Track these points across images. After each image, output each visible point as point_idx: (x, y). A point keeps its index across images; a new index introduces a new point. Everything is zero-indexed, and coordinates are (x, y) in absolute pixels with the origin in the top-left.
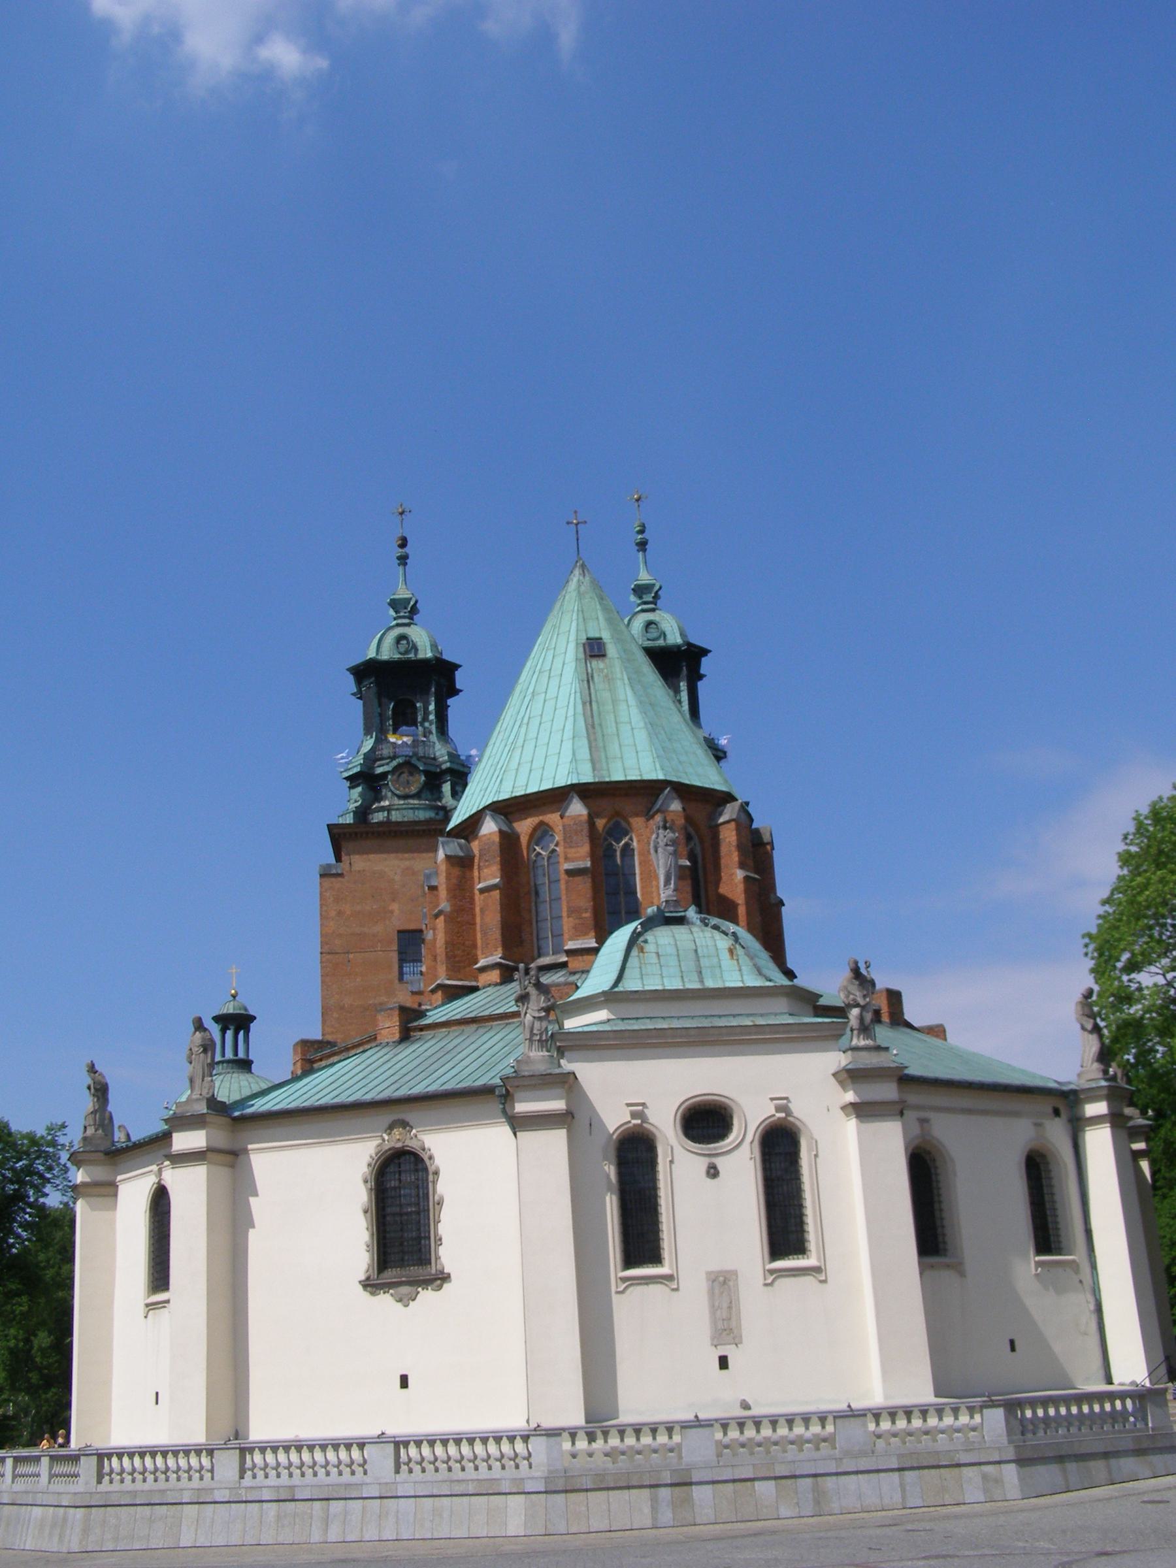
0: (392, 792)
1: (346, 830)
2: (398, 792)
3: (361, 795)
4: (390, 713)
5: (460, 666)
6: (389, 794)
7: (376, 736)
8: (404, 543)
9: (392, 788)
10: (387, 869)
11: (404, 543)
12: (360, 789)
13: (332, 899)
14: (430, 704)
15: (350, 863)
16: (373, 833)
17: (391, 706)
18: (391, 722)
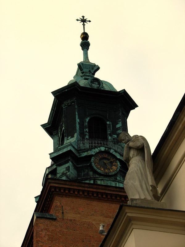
0: (95, 172)
1: (61, 186)
2: (99, 171)
3: (68, 169)
4: (86, 124)
5: (138, 106)
6: (91, 173)
7: (77, 136)
8: (85, 37)
9: (95, 167)
10: (94, 223)
11: (85, 37)
12: (67, 165)
13: (47, 238)
14: (118, 124)
15: (63, 213)
16: (83, 191)
17: (87, 120)
18: (87, 130)
